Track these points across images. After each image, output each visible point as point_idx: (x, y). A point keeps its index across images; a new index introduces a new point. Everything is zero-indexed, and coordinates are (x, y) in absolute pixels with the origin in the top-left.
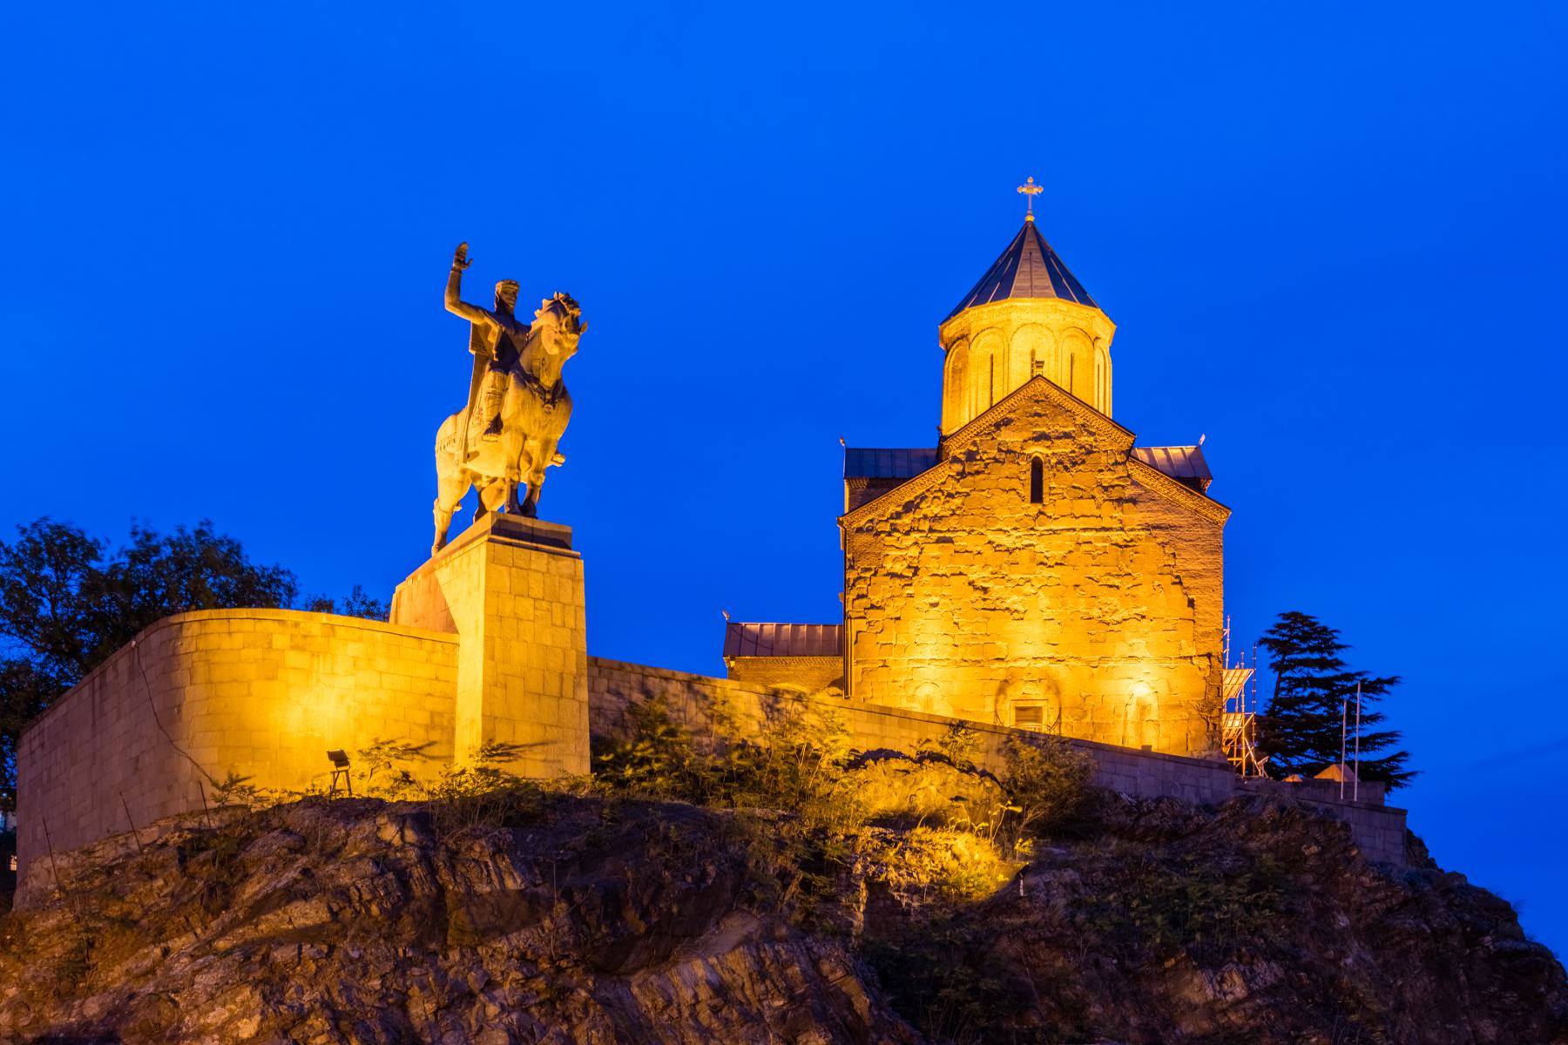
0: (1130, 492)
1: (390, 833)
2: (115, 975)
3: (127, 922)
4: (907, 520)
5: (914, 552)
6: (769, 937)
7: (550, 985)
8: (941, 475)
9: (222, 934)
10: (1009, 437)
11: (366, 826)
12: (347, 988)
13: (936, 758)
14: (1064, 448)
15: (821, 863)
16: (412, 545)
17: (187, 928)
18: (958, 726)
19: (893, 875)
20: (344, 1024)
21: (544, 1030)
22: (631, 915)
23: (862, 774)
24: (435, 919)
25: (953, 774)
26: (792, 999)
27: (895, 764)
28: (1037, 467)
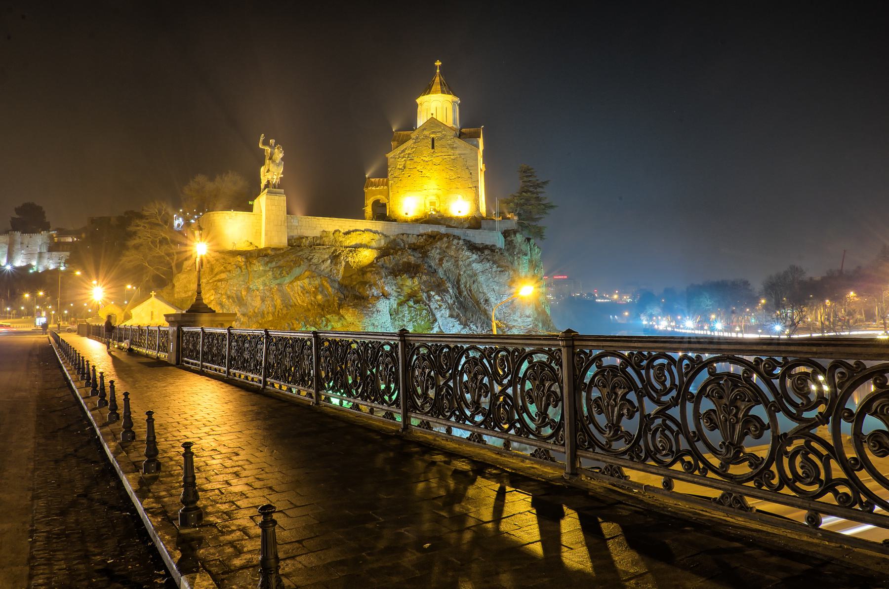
10: (426, 133)
14: (439, 135)
28: (433, 140)
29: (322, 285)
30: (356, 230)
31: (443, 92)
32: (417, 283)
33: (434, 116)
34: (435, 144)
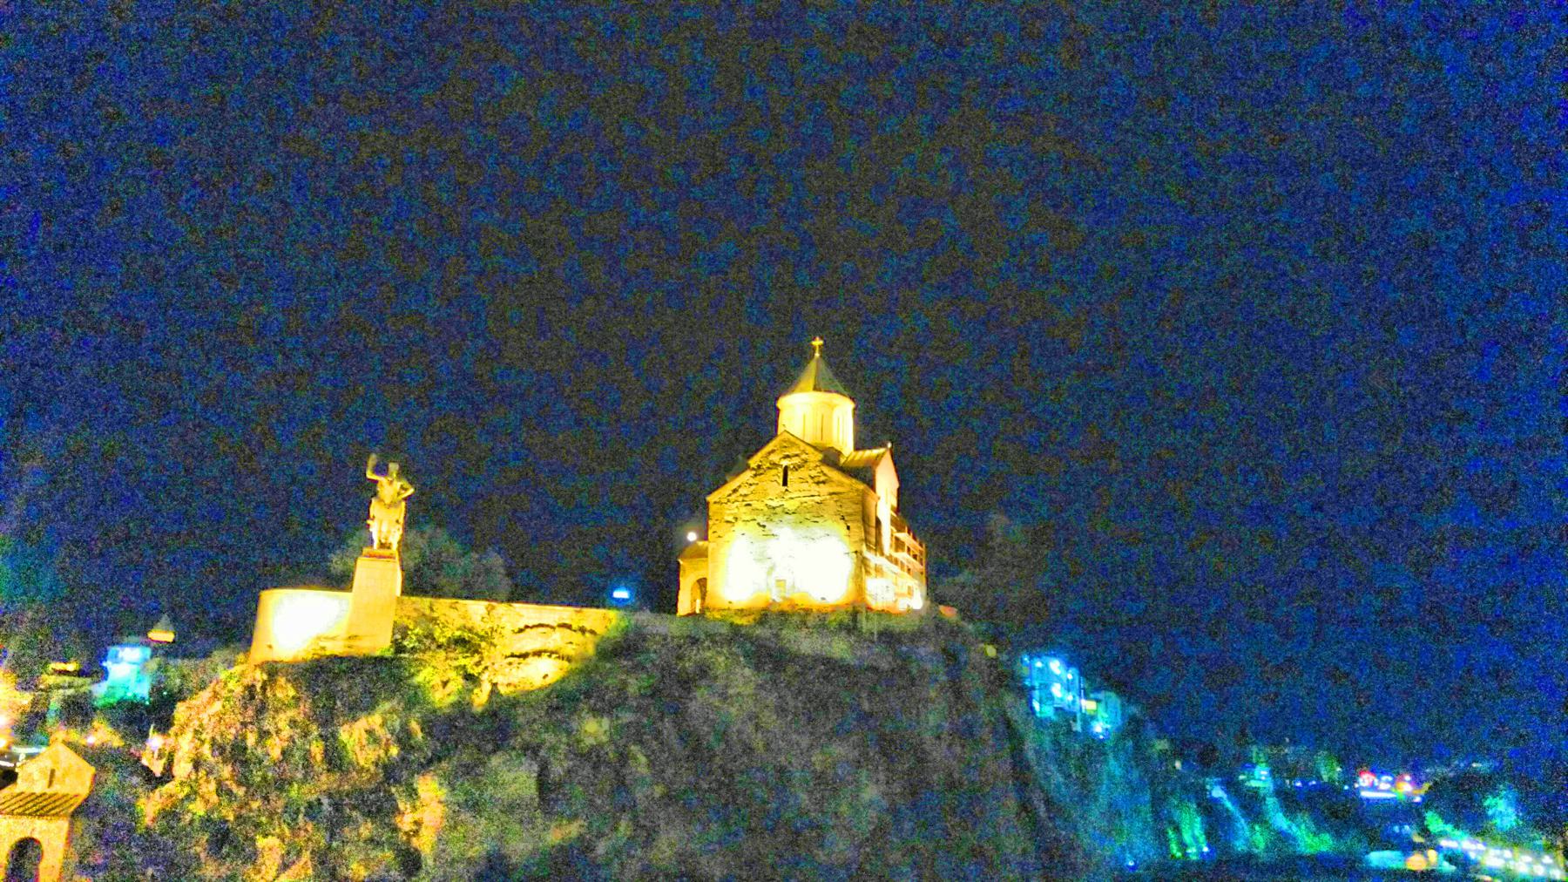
4: (733, 497)
8: (747, 476)
14: (796, 460)
28: (786, 470)
34: (790, 477)
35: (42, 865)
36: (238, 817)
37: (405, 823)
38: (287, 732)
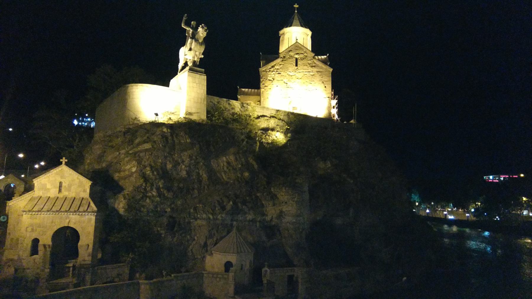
0: (314, 65)
1: (165, 130)
2: (109, 157)
3: (112, 147)
4: (272, 69)
5: (273, 75)
6: (238, 153)
7: (195, 162)
8: (279, 60)
9: (131, 150)
10: (291, 54)
11: (160, 129)
12: (154, 161)
13: (273, 117)
14: (302, 56)
15: (251, 137)
16: (174, 72)
17: (124, 149)
18: (278, 111)
19: (264, 140)
20: (153, 169)
21: (193, 171)
22: (212, 147)
23: (259, 120)
24: (173, 147)
25: (277, 120)
26: (242, 165)
27: (266, 118)
28: (297, 60)
29: (247, 162)
30: (263, 116)
31: (302, 26)
32: (330, 165)
33: (300, 41)
34: (299, 63)
35: (79, 244)
36: (172, 209)
37: (271, 212)
38: (187, 161)
